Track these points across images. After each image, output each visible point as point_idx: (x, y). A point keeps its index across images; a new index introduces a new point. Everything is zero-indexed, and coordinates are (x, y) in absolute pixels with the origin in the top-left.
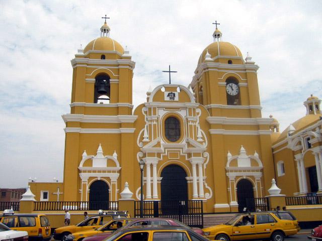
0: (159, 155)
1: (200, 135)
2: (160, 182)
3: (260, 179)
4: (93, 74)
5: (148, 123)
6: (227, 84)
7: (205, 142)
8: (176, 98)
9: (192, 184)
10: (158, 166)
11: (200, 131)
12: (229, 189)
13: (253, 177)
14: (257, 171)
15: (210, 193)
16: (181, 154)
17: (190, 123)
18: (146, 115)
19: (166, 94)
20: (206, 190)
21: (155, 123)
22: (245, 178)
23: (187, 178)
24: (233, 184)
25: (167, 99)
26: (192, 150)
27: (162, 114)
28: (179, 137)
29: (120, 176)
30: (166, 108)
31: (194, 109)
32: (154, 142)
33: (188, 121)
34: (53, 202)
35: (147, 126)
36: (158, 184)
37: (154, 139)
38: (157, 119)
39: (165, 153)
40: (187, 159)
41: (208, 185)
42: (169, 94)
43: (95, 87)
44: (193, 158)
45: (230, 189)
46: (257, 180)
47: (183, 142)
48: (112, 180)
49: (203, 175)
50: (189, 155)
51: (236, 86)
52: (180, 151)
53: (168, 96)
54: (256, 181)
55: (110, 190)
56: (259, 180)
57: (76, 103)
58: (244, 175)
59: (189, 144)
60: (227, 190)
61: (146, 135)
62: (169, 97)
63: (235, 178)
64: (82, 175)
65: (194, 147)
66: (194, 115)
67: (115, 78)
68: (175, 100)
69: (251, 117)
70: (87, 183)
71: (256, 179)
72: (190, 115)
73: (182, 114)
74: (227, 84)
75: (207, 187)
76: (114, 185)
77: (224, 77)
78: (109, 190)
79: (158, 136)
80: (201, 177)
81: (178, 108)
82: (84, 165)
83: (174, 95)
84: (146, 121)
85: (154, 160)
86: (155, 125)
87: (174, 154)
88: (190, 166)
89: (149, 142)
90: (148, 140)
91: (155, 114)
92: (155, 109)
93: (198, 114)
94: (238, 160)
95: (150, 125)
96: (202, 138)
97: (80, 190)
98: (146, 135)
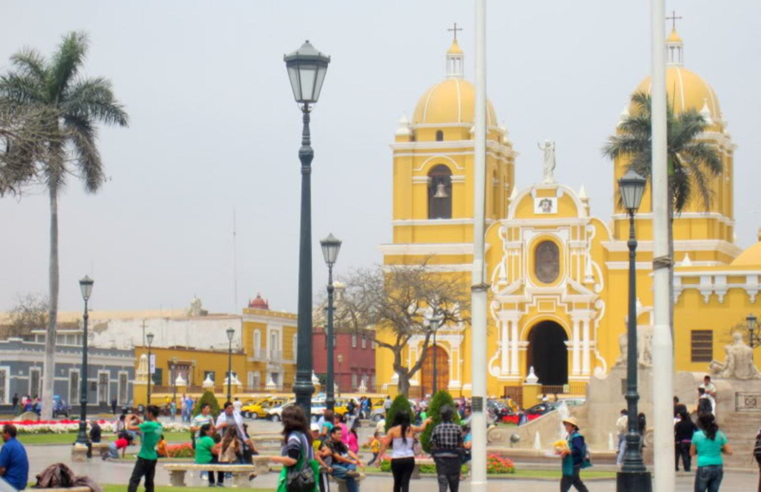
0: (521, 307)
1: (589, 272)
2: (525, 349)
4: (424, 167)
5: (507, 254)
7: (599, 283)
8: (554, 210)
9: (572, 352)
10: (520, 324)
11: (590, 263)
15: (603, 368)
16: (559, 304)
17: (574, 253)
18: (504, 240)
19: (537, 201)
20: (594, 362)
21: (516, 253)
23: (566, 343)
25: (538, 210)
26: (574, 298)
27: (530, 238)
28: (558, 275)
29: (464, 339)
30: (536, 227)
31: (582, 228)
32: (515, 285)
33: (570, 249)
35: (506, 260)
36: (520, 353)
37: (516, 280)
38: (519, 247)
39: (532, 303)
40: (567, 312)
41: (600, 355)
44: (574, 310)
47: (561, 286)
49: (592, 338)
50: (570, 306)
52: (556, 299)
53: (541, 204)
55: (451, 361)
57: (399, 222)
59: (571, 290)
61: (503, 274)
65: (579, 293)
66: (582, 238)
69: (691, 238)
70: (417, 350)
72: (574, 237)
73: (562, 238)
75: (598, 357)
76: (455, 353)
78: (449, 361)
79: (522, 277)
80: (587, 342)
81: (555, 227)
84: (504, 249)
85: (514, 315)
86: (517, 258)
87: (545, 305)
88: (571, 324)
89: (508, 285)
90: (505, 283)
91: (517, 238)
92: (517, 229)
93: (589, 234)
95: (510, 258)
96: (593, 277)
98: (503, 274)
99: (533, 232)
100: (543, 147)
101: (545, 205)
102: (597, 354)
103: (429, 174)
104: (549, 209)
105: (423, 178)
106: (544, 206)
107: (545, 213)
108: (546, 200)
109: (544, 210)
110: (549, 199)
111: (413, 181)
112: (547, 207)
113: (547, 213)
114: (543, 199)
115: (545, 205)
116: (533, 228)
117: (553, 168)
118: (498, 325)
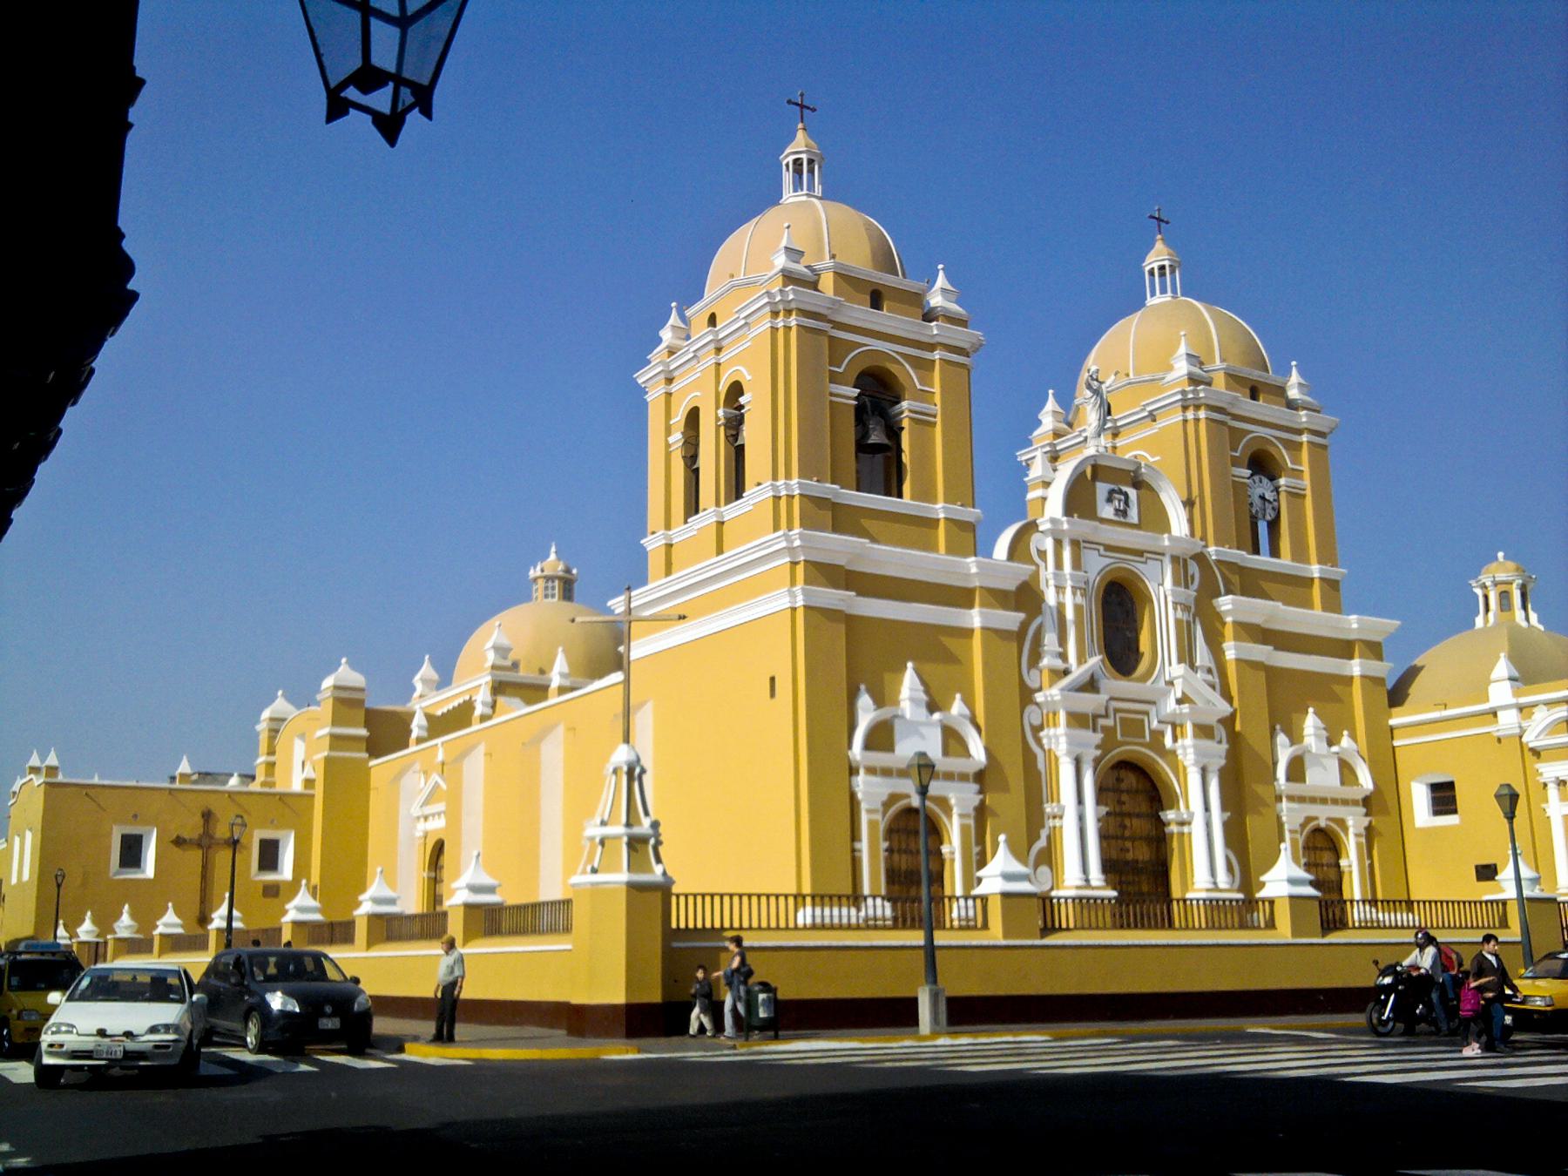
8: (1133, 515)
10: (1097, 761)
16: (1155, 724)
27: (1096, 564)
30: (1109, 548)
34: (1424, 902)
42: (1111, 492)
52: (1147, 713)
53: (1110, 500)
58: (1323, 815)
60: (853, 850)
64: (861, 782)
68: (1129, 520)
78: (945, 849)
82: (868, 745)
89: (1066, 672)
97: (857, 845)
99: (1101, 555)
104: (1124, 513)
108: (1121, 492)
109: (1117, 511)
110: (1124, 489)
111: (832, 394)
114: (1112, 486)
116: (1101, 548)
118: (1041, 765)
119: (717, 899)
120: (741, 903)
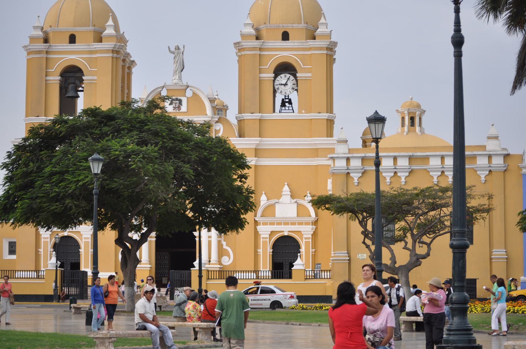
3: (310, 236)
6: (275, 77)
8: (184, 108)
12: (259, 250)
13: (299, 232)
14: (307, 224)
22: (286, 234)
24: (265, 243)
43: (61, 88)
45: (260, 251)
46: (306, 238)
48: (84, 236)
51: (292, 78)
54: (304, 240)
55: (82, 250)
56: (309, 238)
58: (286, 230)
62: (172, 106)
63: (270, 235)
67: (91, 74)
70: (49, 240)
71: (304, 236)
74: (275, 77)
75: (225, 247)
77: (271, 65)
78: (80, 250)
83: (180, 101)
94: (277, 205)
97: (40, 250)
100: (173, 49)
101: (176, 103)
102: (224, 243)
103: (62, 75)
104: (179, 108)
105: (55, 79)
106: (174, 105)
107: (175, 111)
108: (177, 99)
109: (175, 108)
110: (179, 98)
112: (177, 105)
113: (178, 111)
115: (176, 103)
117: (182, 71)
119: (12, 271)
120: (221, 277)
